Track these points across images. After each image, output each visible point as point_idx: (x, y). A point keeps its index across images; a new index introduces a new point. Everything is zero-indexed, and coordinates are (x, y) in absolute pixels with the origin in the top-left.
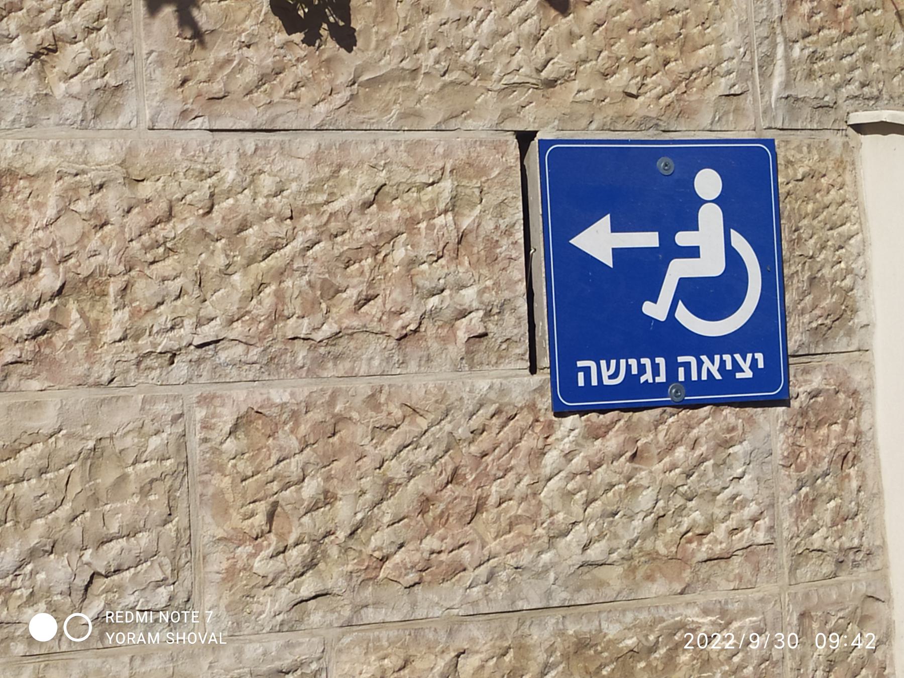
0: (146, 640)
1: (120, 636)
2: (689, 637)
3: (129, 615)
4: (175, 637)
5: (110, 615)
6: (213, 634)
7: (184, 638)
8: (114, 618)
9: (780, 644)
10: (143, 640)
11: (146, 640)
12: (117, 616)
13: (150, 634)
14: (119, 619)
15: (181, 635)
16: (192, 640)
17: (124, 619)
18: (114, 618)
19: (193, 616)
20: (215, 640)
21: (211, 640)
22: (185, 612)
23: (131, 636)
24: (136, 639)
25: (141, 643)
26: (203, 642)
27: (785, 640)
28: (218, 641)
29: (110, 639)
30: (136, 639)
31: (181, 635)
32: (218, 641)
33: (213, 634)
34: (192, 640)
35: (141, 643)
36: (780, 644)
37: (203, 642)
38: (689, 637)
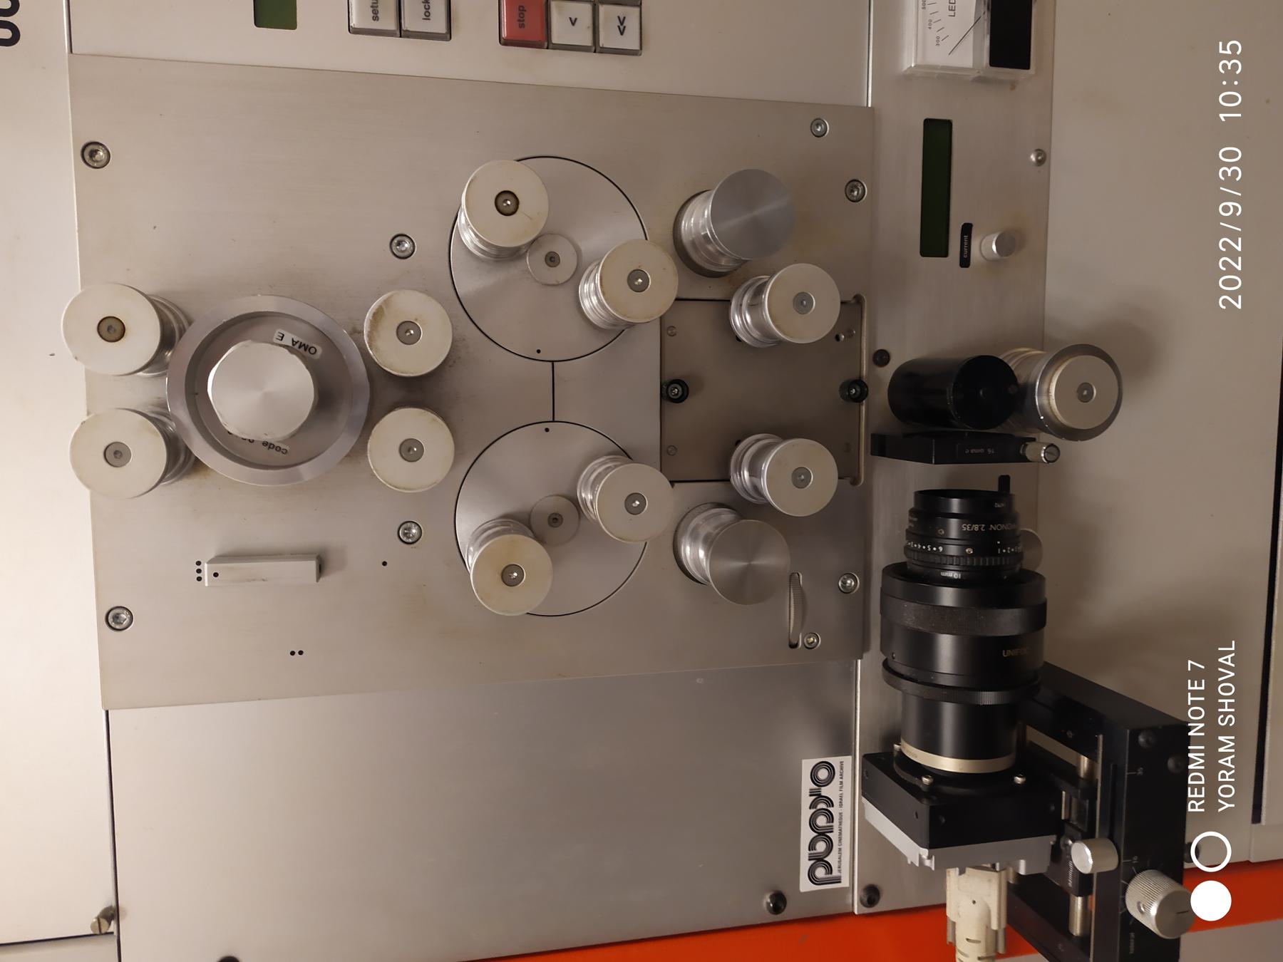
0: (1230, 754)
1: (1224, 791)
2: (1225, 302)
3: (1194, 778)
4: (1226, 714)
5: (1193, 806)
6: (1221, 660)
7: (1226, 701)
8: (1198, 800)
9: (1235, 173)
10: (1229, 758)
11: (1230, 754)
12: (1196, 796)
13: (1221, 750)
14: (1200, 793)
15: (1223, 705)
16: (1229, 689)
17: (1199, 787)
18: (1198, 800)
19: (1196, 688)
20: (1229, 657)
21: (1229, 663)
22: (1190, 699)
23: (1223, 776)
24: (1229, 769)
25: (1233, 761)
26: (1232, 674)
27: (1229, 165)
28: (1230, 652)
29: (1227, 805)
30: (1229, 769)
31: (1223, 705)
32: (1230, 652)
33: (1221, 660)
34: (1229, 689)
35: (1233, 761)
36: (1235, 173)
37: (1232, 674)
38: (1225, 302)
